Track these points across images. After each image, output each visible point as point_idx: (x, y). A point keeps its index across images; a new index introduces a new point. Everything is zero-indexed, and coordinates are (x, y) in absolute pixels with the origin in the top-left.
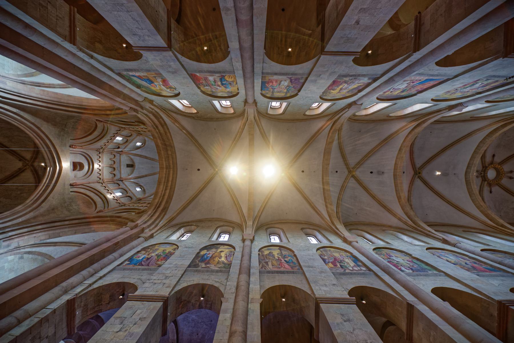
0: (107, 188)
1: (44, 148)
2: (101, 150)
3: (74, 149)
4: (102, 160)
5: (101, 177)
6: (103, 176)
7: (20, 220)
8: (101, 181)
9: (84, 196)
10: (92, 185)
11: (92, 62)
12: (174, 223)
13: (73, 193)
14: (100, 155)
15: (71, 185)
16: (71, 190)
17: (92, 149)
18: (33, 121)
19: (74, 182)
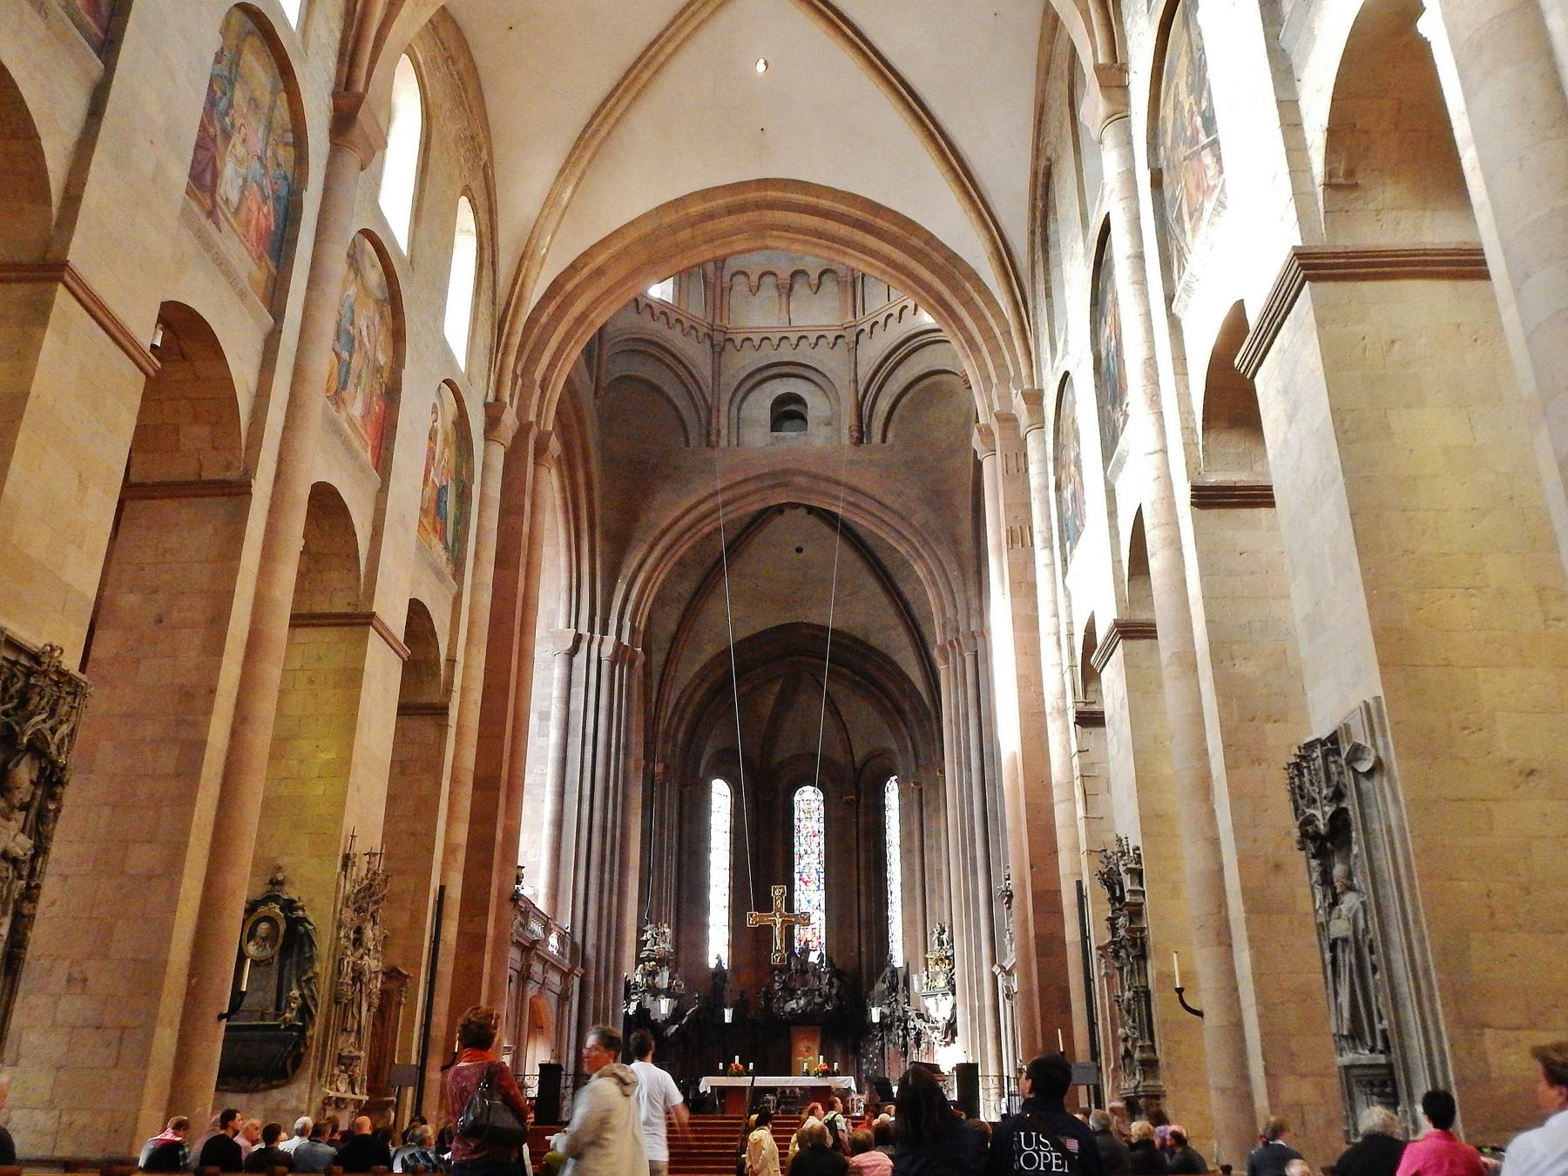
0: (881, 319)
2: (719, 338)
3: (724, 432)
4: (758, 330)
5: (831, 337)
6: (829, 328)
8: (850, 336)
9: (904, 401)
10: (865, 371)
11: (460, 657)
12: (1023, 260)
13: (890, 435)
14: (738, 339)
15: (859, 441)
16: (877, 438)
17: (717, 373)
18: (645, 548)
19: (846, 431)
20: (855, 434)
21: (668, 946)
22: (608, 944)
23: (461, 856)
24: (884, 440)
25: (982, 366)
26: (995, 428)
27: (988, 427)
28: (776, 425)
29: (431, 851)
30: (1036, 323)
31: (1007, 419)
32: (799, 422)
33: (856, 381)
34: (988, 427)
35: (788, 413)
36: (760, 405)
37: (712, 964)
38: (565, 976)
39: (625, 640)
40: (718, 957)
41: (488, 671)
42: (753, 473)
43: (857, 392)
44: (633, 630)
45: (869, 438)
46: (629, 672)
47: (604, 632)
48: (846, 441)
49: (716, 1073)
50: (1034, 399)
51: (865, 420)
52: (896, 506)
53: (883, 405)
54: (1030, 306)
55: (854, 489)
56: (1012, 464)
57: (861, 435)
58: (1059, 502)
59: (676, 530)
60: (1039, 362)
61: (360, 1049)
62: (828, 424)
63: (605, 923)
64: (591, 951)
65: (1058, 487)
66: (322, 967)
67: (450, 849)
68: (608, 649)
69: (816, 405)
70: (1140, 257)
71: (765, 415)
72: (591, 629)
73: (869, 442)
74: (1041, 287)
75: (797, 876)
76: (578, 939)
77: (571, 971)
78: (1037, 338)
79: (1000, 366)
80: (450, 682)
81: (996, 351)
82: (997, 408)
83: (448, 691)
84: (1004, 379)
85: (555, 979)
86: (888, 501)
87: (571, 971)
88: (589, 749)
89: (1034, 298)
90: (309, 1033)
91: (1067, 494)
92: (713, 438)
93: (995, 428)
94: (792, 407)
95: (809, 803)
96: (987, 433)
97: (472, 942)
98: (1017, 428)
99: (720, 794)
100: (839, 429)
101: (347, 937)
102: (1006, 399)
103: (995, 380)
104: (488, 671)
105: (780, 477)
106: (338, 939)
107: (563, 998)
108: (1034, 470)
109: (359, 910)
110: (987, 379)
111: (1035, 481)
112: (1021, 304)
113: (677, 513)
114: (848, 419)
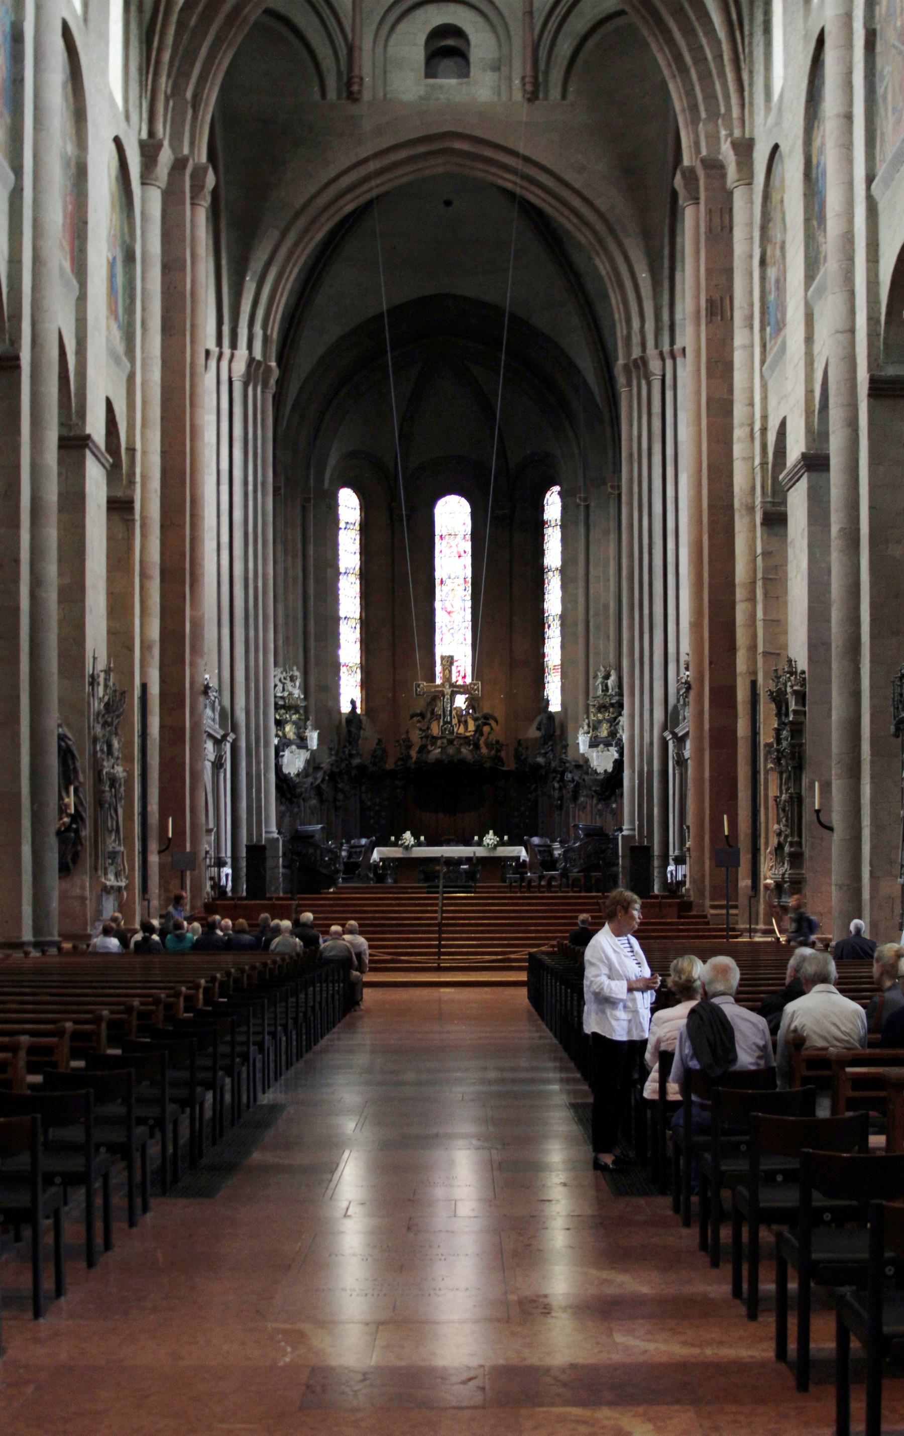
1: (371, 189)
7: (644, 276)
9: (590, 44)
11: (138, 446)
16: (555, 93)
19: (517, 82)
20: (529, 88)
21: (297, 693)
22: (257, 707)
23: (156, 651)
24: (564, 96)
25: (690, 93)
26: (701, 173)
27: (692, 170)
28: (431, 71)
29: (131, 649)
30: (751, 53)
31: (715, 167)
32: (460, 60)
33: (530, 13)
34: (692, 170)
35: (447, 49)
36: (411, 41)
37: (345, 708)
38: (218, 742)
39: (258, 354)
40: (353, 703)
41: (164, 454)
42: (403, 137)
43: (532, 30)
44: (266, 340)
45: (546, 92)
46: (263, 392)
47: (234, 346)
48: (518, 96)
49: (386, 843)
50: (744, 148)
51: (542, 66)
52: (577, 186)
53: (565, 48)
54: (746, 43)
55: (527, 160)
56: (717, 220)
57: (535, 92)
58: (763, 278)
59: (312, 211)
60: (751, 104)
61: (119, 845)
62: (496, 68)
63: (252, 685)
64: (241, 716)
65: (763, 262)
66: (85, 777)
67: (146, 647)
68: (240, 367)
69: (481, 43)
70: (849, 117)
71: (418, 54)
72: (219, 343)
73: (546, 98)
74: (759, 17)
75: (438, 605)
76: (227, 703)
77: (224, 737)
78: (751, 72)
79: (710, 97)
80: (132, 474)
81: (706, 78)
82: (704, 152)
83: (132, 482)
84: (714, 114)
85: (209, 746)
86: (569, 177)
87: (224, 737)
88: (225, 488)
89: (751, 21)
90: (83, 834)
91: (772, 272)
92: (355, 88)
93: (701, 173)
94: (450, 42)
95: (453, 516)
96: (690, 177)
97: (173, 734)
98: (724, 176)
99: (349, 504)
100: (510, 79)
101: (102, 750)
102: (714, 139)
103: (703, 115)
104: (163, 453)
105: (437, 143)
106: (95, 752)
107: (218, 765)
108: (738, 234)
109: (105, 724)
110: (694, 108)
111: (739, 248)
112: (736, 27)
113: (313, 189)
114: (519, 68)
